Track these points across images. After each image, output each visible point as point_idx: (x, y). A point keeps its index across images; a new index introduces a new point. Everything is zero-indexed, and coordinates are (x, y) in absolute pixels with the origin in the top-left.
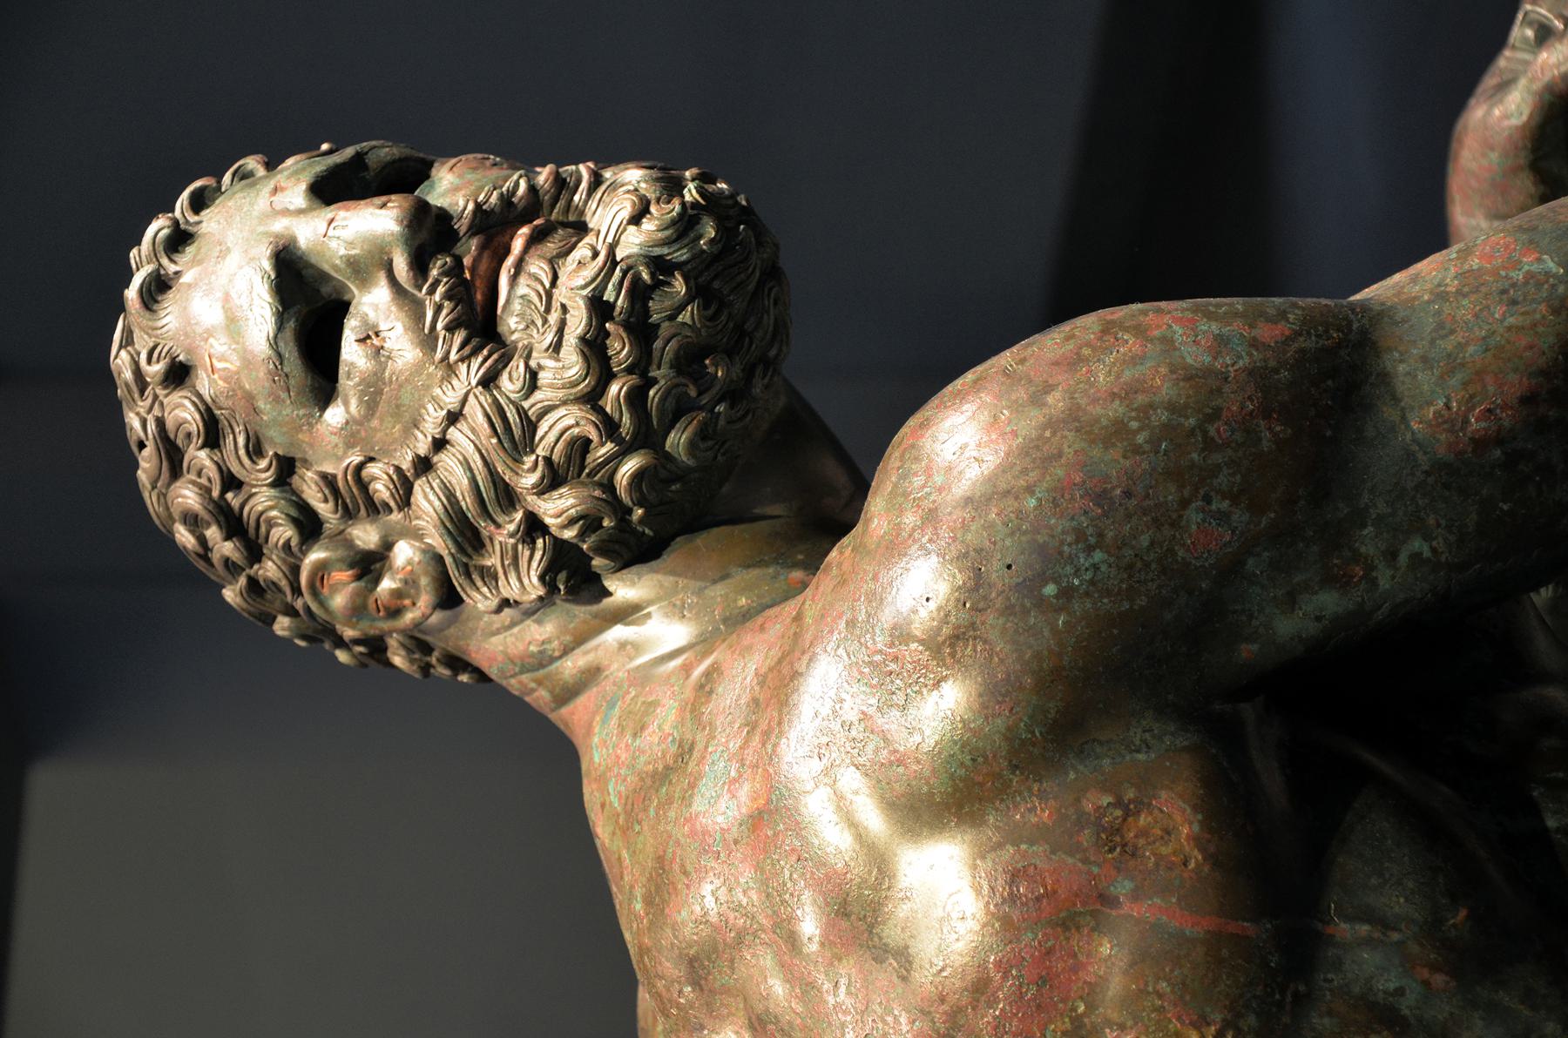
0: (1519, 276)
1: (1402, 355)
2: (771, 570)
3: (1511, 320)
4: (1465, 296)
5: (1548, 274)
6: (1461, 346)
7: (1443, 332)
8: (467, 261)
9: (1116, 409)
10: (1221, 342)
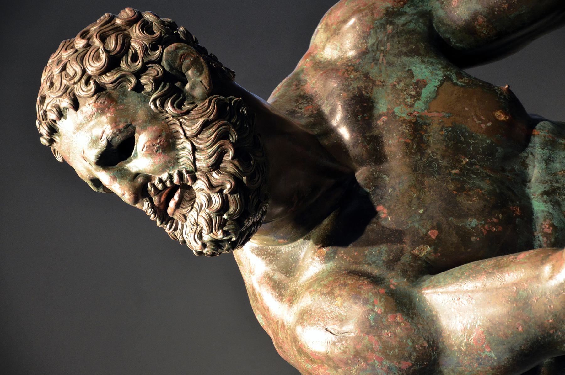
1: (446, 367)
2: (273, 238)
3: (479, 369)
4: (467, 355)
7: (459, 365)
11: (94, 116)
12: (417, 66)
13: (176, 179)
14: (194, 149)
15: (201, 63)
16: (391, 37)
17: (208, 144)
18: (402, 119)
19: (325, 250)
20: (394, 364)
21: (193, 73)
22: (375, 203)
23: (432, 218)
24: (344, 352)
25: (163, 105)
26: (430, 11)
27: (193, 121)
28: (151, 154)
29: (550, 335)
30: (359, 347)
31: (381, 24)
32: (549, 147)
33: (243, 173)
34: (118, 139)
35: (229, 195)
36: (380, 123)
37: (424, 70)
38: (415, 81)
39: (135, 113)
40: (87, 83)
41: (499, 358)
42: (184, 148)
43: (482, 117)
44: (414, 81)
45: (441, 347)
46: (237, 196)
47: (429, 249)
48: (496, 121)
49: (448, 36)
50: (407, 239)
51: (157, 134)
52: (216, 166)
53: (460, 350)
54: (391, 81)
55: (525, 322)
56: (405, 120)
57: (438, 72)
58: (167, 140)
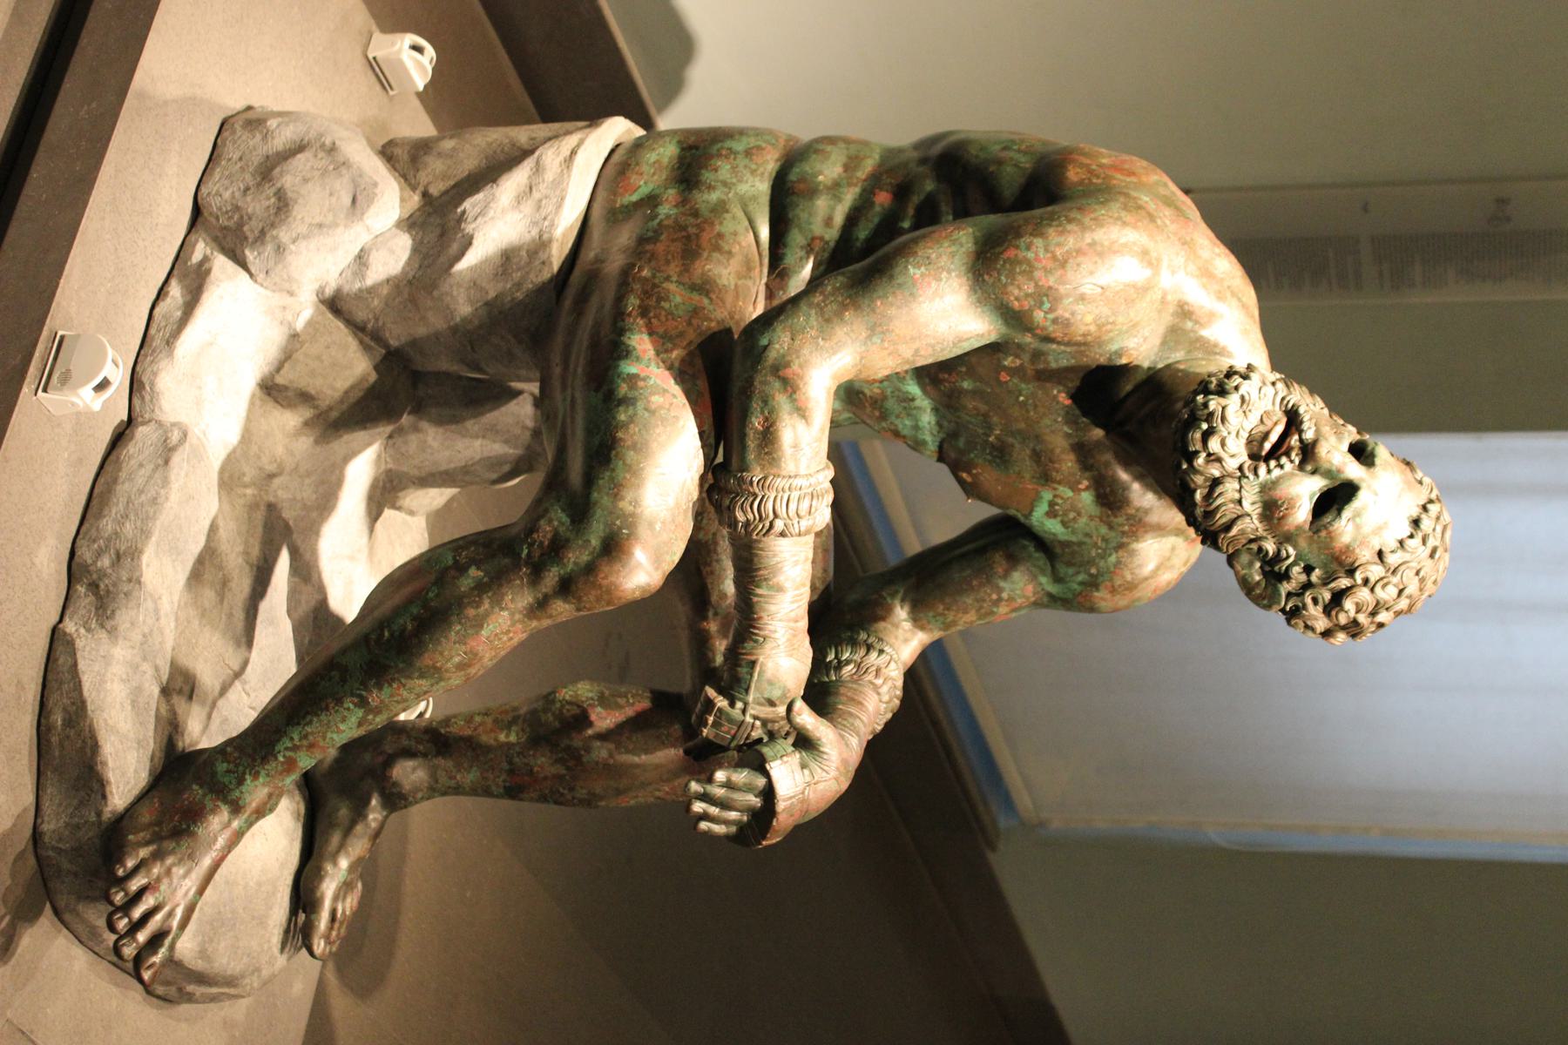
0: (923, 269)
5: (914, 268)
6: (950, 246)
8: (1296, 437)
9: (1069, 227)
10: (1028, 248)
11: (1358, 543)
13: (1262, 469)
14: (1240, 502)
16: (1091, 562)
17: (1224, 508)
19: (1124, 361)
20: (1022, 254)
21: (1253, 579)
22: (1074, 406)
23: (1010, 392)
24: (1078, 265)
27: (1242, 532)
28: (1292, 499)
29: (850, 297)
30: (1059, 272)
31: (1102, 576)
33: (1185, 472)
34: (1328, 518)
35: (1201, 449)
36: (1086, 483)
39: (1310, 544)
41: (906, 267)
42: (1253, 504)
44: (1059, 519)
45: (970, 275)
46: (1192, 449)
47: (1006, 363)
48: (969, 473)
49: (1037, 555)
50: (1030, 373)
51: (1283, 522)
52: (1216, 482)
53: (949, 272)
54: (1083, 520)
55: (873, 311)
58: (1273, 513)
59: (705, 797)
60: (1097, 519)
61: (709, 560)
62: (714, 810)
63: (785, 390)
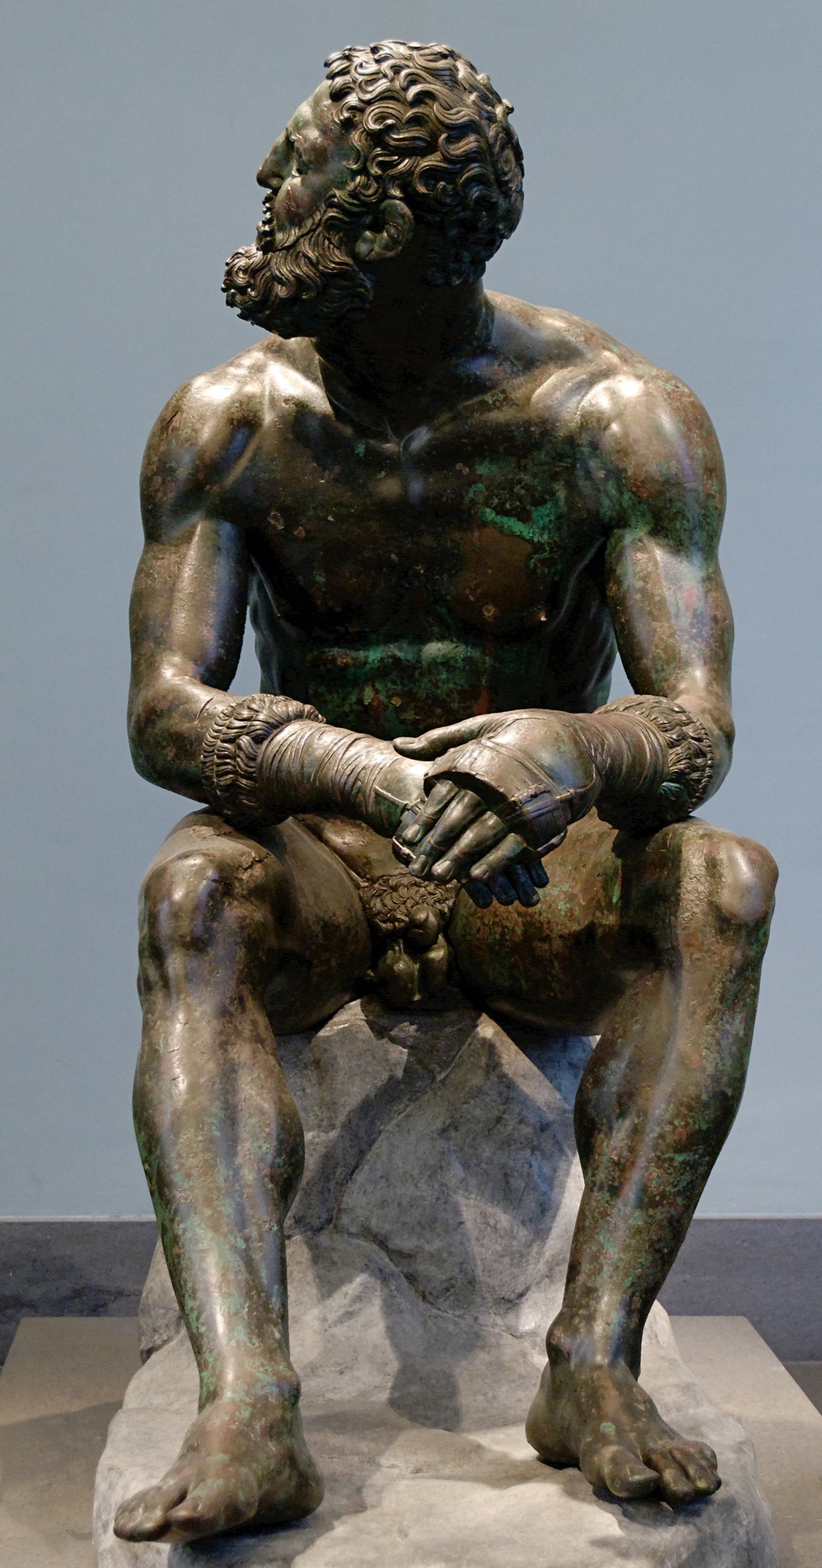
12: (553, 510)
14: (288, 248)
15: (396, 248)
18: (464, 493)
25: (331, 205)
26: (630, 526)
27: (315, 245)
32: (467, 668)
36: (459, 466)
37: (547, 520)
38: (528, 507)
40: (352, 108)
43: (478, 591)
47: (280, 527)
54: (526, 478)
56: (463, 497)
57: (546, 537)
59: (437, 854)
60: (523, 462)
61: (538, 925)
62: (455, 851)
63: (154, 723)
